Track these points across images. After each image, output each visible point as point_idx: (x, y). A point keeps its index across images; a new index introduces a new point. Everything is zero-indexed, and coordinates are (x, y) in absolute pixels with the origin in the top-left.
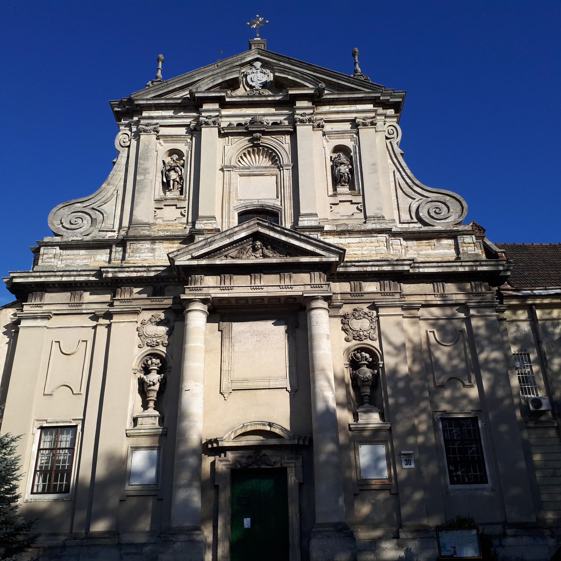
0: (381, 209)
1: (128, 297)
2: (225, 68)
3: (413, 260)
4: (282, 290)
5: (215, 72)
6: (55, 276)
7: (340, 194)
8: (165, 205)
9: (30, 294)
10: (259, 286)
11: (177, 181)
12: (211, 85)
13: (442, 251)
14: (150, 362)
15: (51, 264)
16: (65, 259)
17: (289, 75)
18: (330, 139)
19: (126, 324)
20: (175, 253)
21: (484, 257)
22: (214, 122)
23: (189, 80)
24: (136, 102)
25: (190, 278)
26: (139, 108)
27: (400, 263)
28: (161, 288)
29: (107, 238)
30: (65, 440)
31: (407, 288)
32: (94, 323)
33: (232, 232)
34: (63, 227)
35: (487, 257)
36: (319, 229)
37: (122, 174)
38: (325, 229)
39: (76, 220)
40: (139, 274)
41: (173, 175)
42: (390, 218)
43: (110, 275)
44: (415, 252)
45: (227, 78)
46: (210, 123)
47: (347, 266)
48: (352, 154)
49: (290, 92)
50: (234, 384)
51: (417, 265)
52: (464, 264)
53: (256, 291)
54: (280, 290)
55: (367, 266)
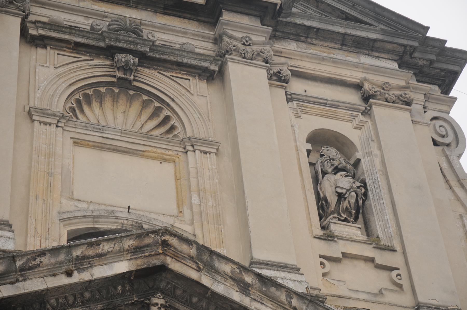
18: (303, 113)
33: (91, 252)
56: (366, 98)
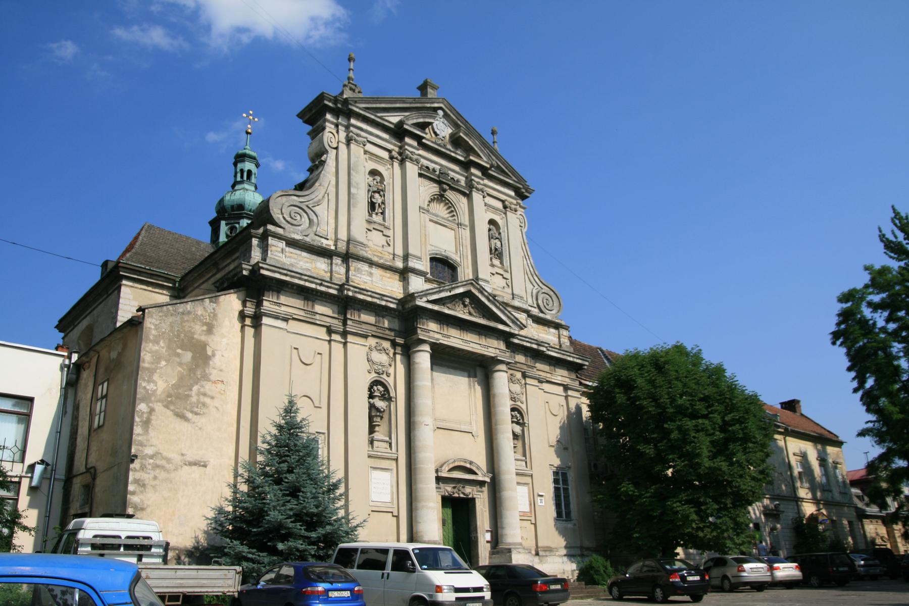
6: (300, 279)
14: (375, 388)
24: (350, 107)
34: (284, 218)
43: (350, 294)
49: (471, 158)
56: (505, 207)
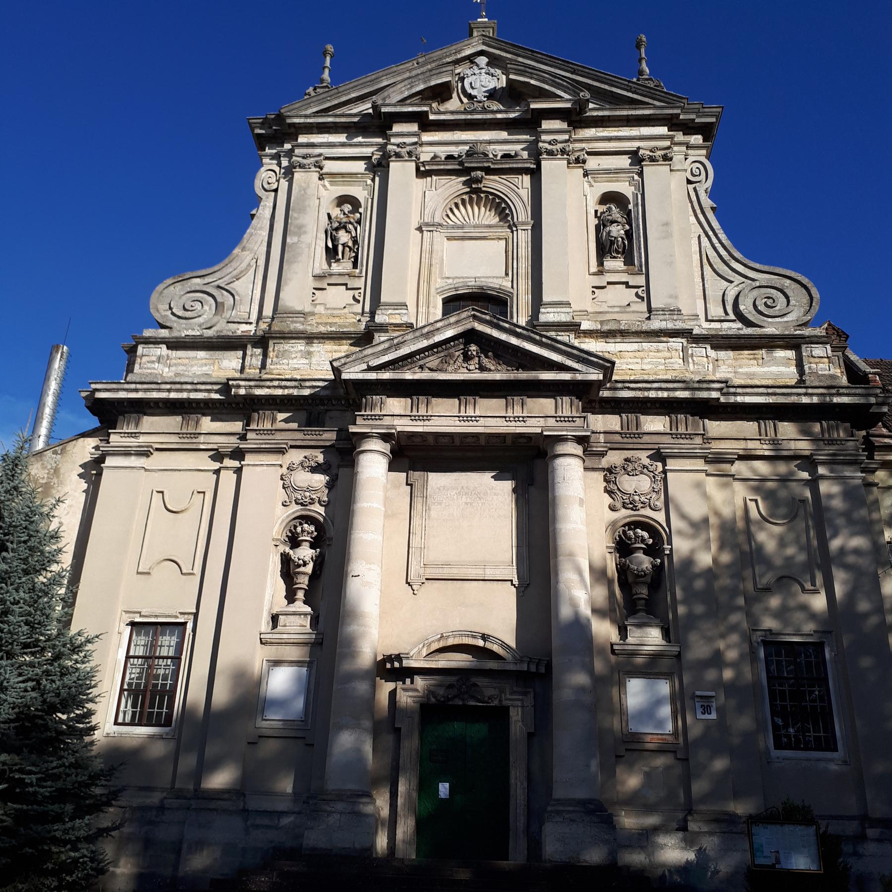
0: (676, 297)
1: (269, 427)
2: (429, 67)
3: (727, 382)
4: (509, 424)
5: (414, 73)
6: (159, 390)
7: (609, 271)
8: (329, 284)
9: (121, 417)
10: (471, 417)
11: (348, 246)
12: (406, 94)
13: (774, 369)
14: (299, 529)
15: (153, 371)
16: (175, 365)
17: (531, 78)
18: (595, 181)
19: (265, 468)
20: (343, 361)
21: (844, 380)
22: (410, 154)
23: (373, 85)
24: (289, 121)
25: (364, 400)
26: (293, 130)
27: (705, 386)
28: (319, 414)
29: (239, 333)
30: (167, 644)
31: (715, 427)
32: (217, 465)
33: (432, 329)
34: (173, 314)
35: (850, 380)
36: (573, 327)
37: (265, 233)
38: (582, 328)
39: (193, 304)
40: (286, 392)
41: (344, 237)
42: (691, 313)
43: (242, 392)
44: (730, 370)
45: (433, 83)
46: (403, 154)
47: (616, 389)
48: (631, 207)
49: (533, 106)
50: (428, 570)
51: (732, 390)
52: (810, 391)
53: (467, 423)
54: (506, 424)
55: (650, 389)
